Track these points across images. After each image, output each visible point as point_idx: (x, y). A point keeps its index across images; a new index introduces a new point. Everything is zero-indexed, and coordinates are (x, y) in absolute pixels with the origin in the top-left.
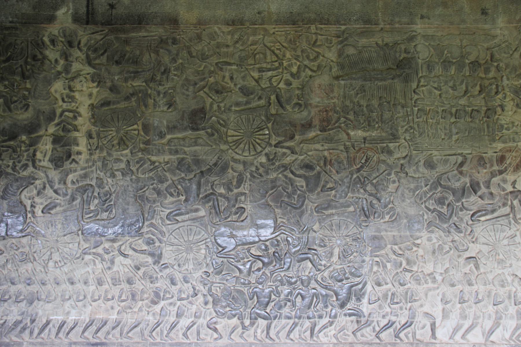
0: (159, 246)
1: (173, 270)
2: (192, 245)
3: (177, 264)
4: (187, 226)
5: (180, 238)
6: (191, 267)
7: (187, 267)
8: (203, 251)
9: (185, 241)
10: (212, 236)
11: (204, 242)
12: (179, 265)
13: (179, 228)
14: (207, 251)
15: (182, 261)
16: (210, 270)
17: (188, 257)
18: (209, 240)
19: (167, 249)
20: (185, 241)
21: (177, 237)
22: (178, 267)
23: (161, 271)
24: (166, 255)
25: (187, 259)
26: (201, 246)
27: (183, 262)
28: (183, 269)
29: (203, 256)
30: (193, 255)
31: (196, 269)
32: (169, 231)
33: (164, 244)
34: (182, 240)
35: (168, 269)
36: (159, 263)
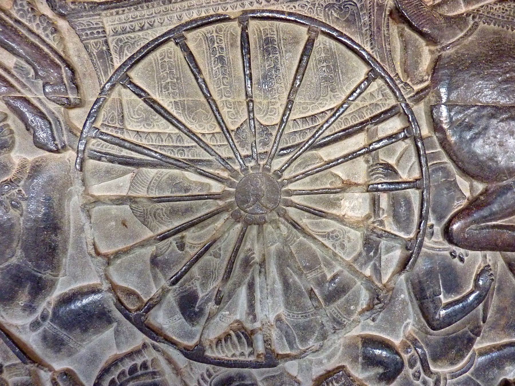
0: (36, 169)
1: (141, 338)
2: (277, 164)
3: (171, 298)
4: (243, 20)
5: (190, 110)
6: (272, 310)
7: (240, 312)
8: (354, 206)
9: (225, 131)
10: (419, 97)
11: (359, 141)
12: (189, 307)
13: (177, 35)
14: (384, 201)
15: (207, 275)
16: (393, 330)
17: (254, 247)
18: (395, 125)
19: (98, 189)
20: (225, 131)
21: (166, 103)
22: (179, 318)
23: (56, 344)
24: (89, 234)
25: (247, 263)
26: (338, 171)
27: (214, 285)
28: (212, 335)
29: (356, 236)
30: (284, 229)
31: (305, 331)
32: (105, 56)
33: (70, 155)
34: (206, 127)
35: (109, 333)
36: (39, 288)
